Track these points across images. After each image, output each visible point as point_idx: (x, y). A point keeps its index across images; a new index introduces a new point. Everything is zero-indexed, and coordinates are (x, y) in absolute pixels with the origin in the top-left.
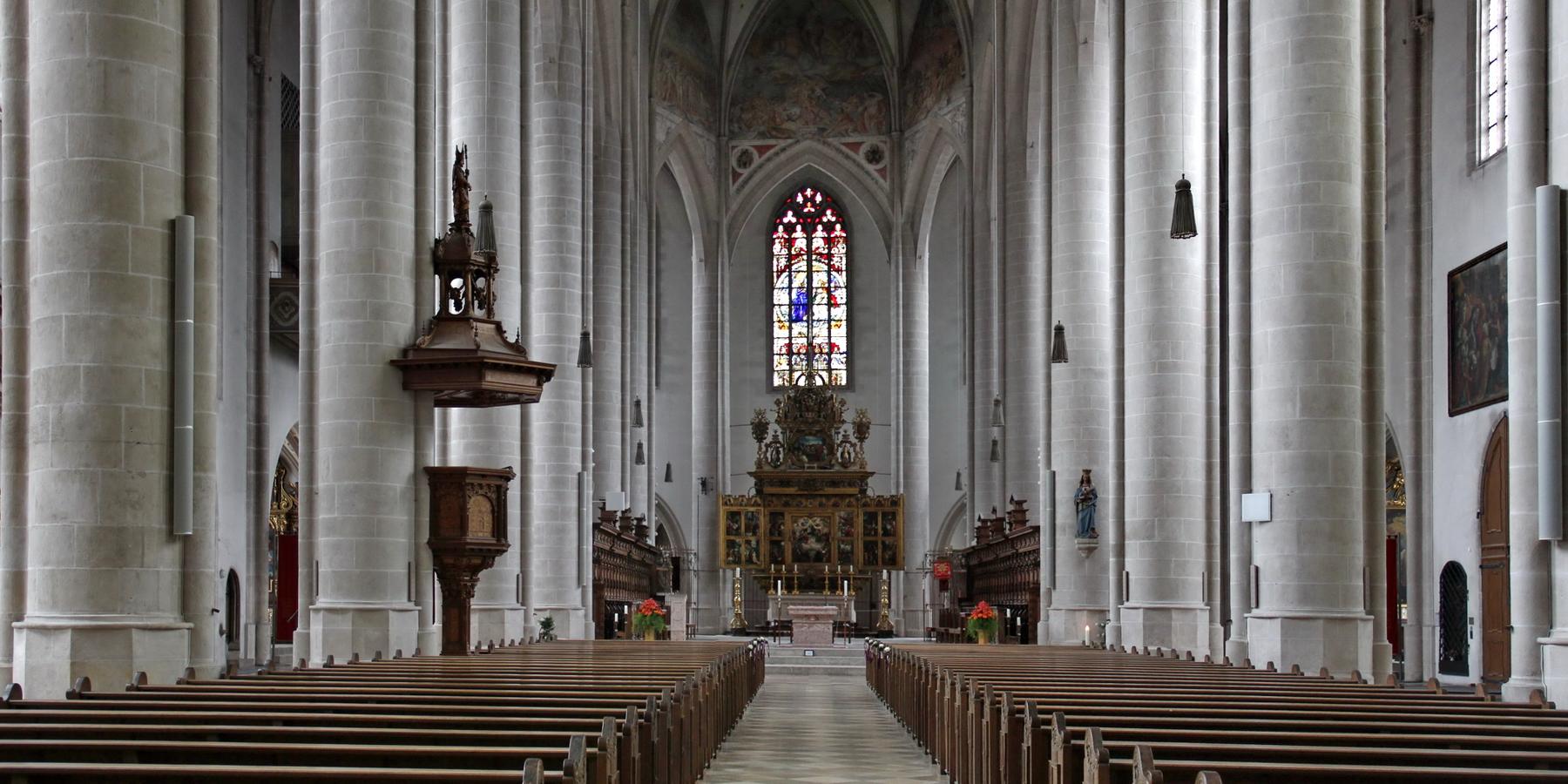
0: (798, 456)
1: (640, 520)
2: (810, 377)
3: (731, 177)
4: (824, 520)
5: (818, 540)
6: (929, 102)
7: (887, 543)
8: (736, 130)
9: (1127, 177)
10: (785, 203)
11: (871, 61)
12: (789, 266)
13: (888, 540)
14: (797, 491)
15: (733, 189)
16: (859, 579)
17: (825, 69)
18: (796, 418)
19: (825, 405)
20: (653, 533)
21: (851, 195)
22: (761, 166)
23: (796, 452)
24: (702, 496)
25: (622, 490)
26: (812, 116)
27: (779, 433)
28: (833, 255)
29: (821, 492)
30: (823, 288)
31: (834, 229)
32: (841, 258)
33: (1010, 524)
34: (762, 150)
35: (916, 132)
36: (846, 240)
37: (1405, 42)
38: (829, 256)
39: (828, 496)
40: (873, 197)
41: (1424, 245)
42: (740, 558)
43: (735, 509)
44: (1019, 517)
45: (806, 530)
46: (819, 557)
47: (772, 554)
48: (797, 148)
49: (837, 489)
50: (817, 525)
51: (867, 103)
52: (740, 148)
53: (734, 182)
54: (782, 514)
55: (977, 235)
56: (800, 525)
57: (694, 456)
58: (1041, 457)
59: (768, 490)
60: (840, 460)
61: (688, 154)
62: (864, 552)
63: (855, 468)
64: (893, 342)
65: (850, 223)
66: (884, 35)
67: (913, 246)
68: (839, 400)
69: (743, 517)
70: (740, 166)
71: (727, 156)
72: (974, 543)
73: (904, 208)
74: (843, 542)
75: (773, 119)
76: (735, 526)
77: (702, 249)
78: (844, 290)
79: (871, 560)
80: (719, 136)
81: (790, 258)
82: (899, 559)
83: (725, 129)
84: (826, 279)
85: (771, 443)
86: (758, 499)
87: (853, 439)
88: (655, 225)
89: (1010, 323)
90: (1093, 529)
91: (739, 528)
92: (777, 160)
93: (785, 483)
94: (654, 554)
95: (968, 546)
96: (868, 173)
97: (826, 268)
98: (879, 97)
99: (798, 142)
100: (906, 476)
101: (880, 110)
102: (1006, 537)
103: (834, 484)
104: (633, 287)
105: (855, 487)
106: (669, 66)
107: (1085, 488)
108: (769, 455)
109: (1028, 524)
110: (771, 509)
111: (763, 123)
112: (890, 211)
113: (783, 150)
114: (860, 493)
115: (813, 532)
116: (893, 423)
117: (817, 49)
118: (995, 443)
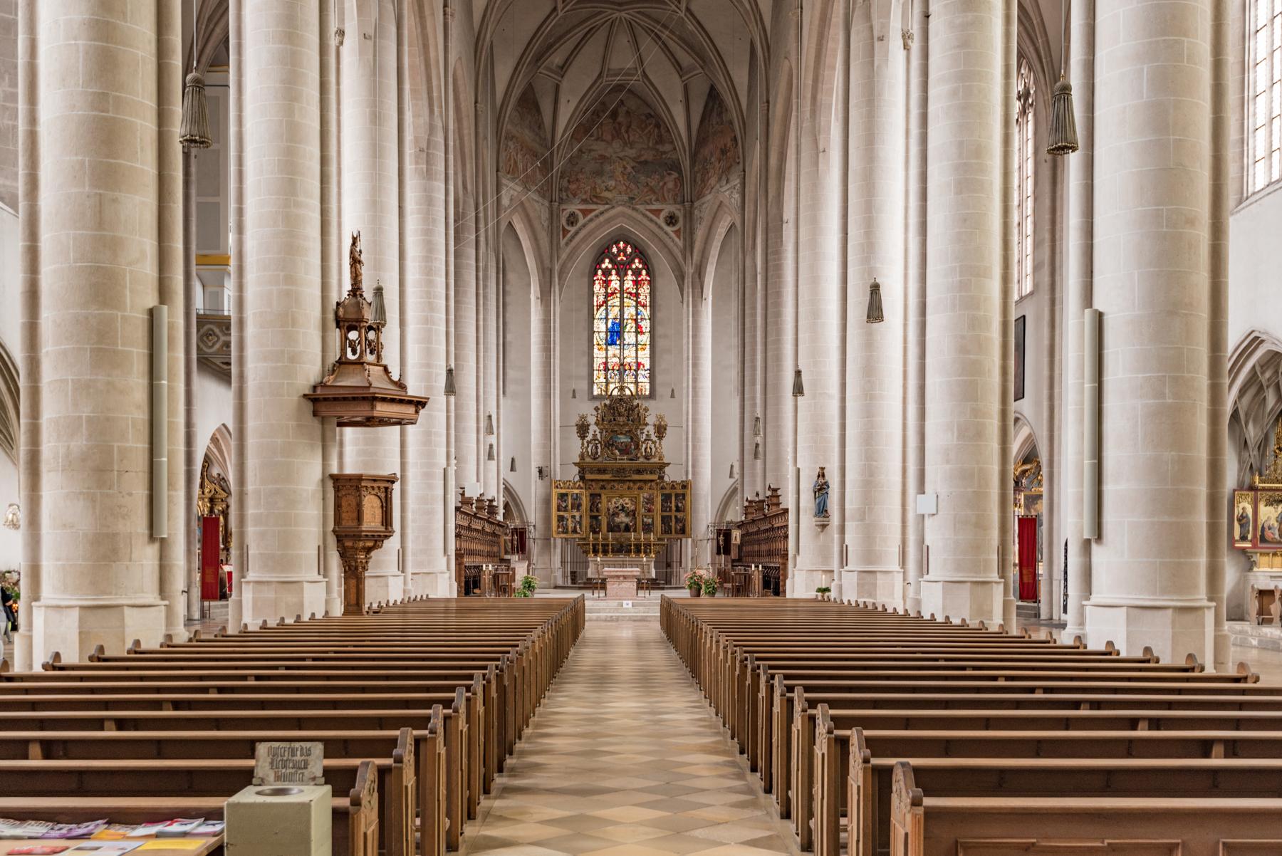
1: (491, 501)
2: (622, 389)
3: (561, 233)
5: (627, 515)
6: (713, 181)
8: (565, 197)
9: (849, 258)
11: (667, 147)
13: (680, 515)
15: (563, 242)
17: (632, 152)
18: (611, 421)
19: (633, 410)
20: (501, 511)
21: (653, 249)
22: (584, 226)
24: (539, 481)
25: (478, 481)
26: (625, 188)
27: (597, 433)
29: (629, 478)
33: (768, 505)
34: (585, 213)
35: (703, 204)
37: (1046, 161)
39: (635, 482)
40: (671, 252)
41: (1057, 308)
42: (567, 529)
43: (564, 491)
44: (774, 500)
45: (617, 507)
46: (627, 529)
47: (591, 526)
48: (613, 212)
51: (667, 179)
52: (569, 211)
53: (564, 237)
54: (600, 495)
55: (748, 284)
57: (532, 450)
58: (790, 457)
59: (588, 476)
61: (527, 216)
63: (656, 460)
64: (685, 363)
66: (677, 128)
68: (644, 407)
70: (568, 224)
71: (558, 216)
72: (743, 518)
73: (694, 261)
74: (646, 516)
75: (594, 189)
76: (564, 505)
77: (538, 289)
79: (667, 530)
80: (551, 201)
83: (556, 196)
85: (591, 440)
86: (581, 483)
87: (654, 438)
88: (502, 271)
89: (770, 354)
90: (826, 511)
91: (567, 506)
92: (597, 221)
93: (602, 471)
94: (503, 526)
95: (739, 520)
96: (666, 233)
98: (675, 175)
99: (613, 207)
100: (693, 466)
101: (676, 185)
102: (764, 515)
103: (639, 472)
104: (485, 320)
106: (512, 147)
107: (821, 480)
108: (589, 449)
109: (781, 507)
110: (591, 491)
111: (586, 192)
113: (602, 213)
114: (659, 479)
115: (623, 509)
116: (684, 426)
117: (626, 136)
118: (757, 445)
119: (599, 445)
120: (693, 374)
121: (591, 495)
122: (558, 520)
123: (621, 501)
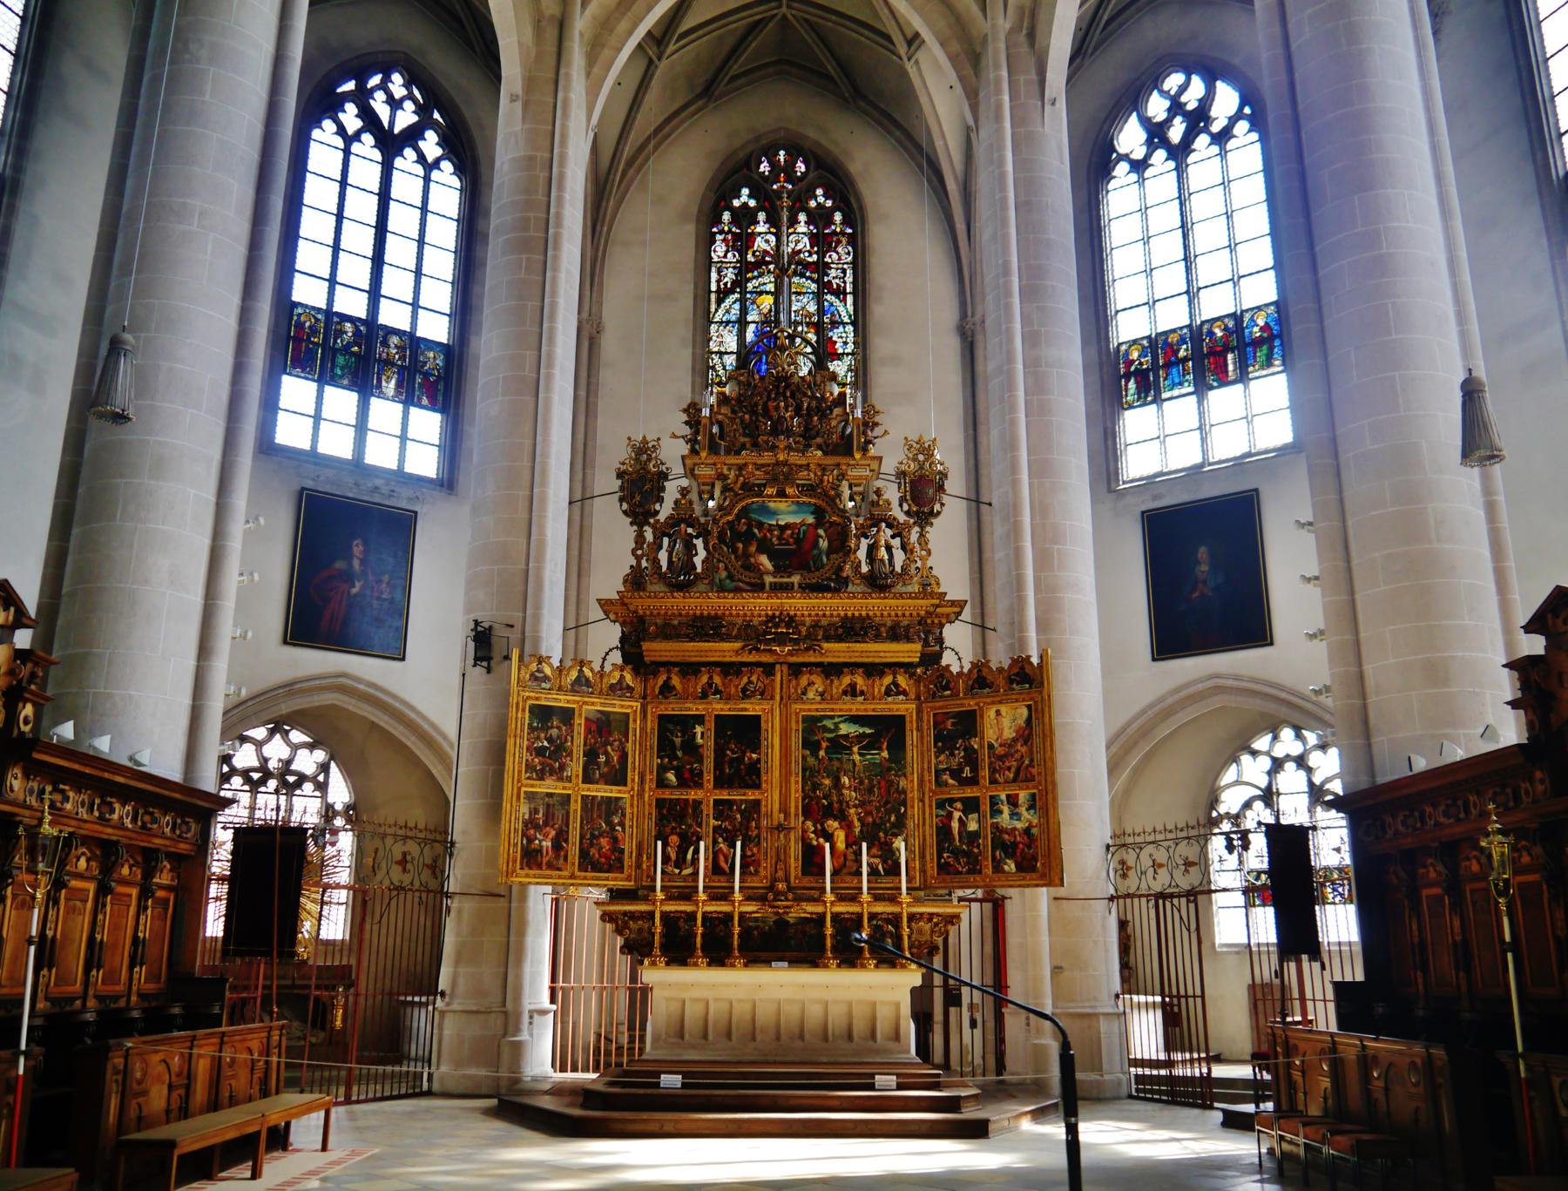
0: (746, 555)
10: (735, 171)
12: (740, 283)
14: (737, 652)
23: (740, 545)
28: (827, 266)
29: (811, 658)
30: (808, 324)
31: (831, 222)
32: (844, 271)
36: (852, 240)
38: (821, 268)
49: (859, 647)
59: (656, 649)
60: (865, 569)
65: (862, 208)
67: (1034, 76)
78: (850, 328)
81: (744, 269)
84: (812, 308)
85: (674, 521)
86: (628, 678)
87: (902, 518)
93: (707, 627)
97: (814, 287)
100: (1043, 626)
105: (909, 640)
108: (663, 556)
112: (980, 15)
119: (699, 543)
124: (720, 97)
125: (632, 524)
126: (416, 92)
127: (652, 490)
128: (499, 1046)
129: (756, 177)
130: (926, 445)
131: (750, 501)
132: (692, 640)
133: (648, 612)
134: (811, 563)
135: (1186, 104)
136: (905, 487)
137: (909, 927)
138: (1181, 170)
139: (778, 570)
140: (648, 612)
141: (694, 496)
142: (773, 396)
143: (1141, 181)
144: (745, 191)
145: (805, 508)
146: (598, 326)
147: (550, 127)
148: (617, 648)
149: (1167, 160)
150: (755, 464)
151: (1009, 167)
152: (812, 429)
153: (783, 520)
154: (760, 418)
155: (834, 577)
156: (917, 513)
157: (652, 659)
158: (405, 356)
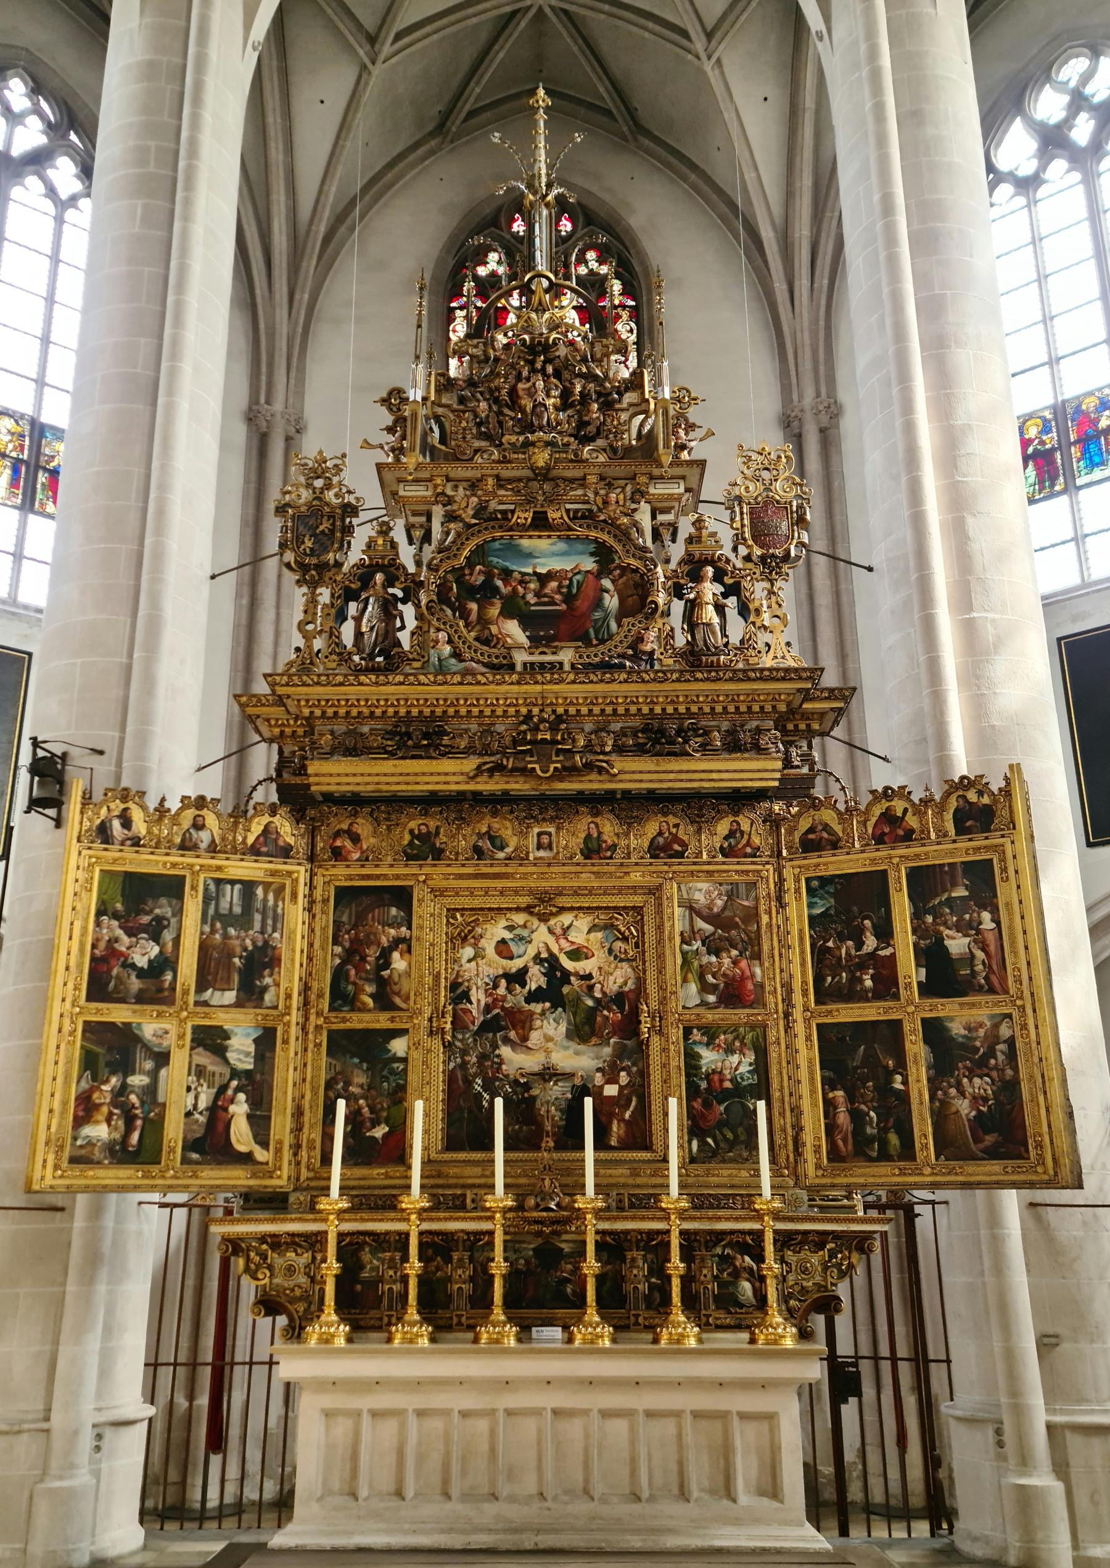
0: (484, 622)
4: (609, 927)
7: (957, 1029)
16: (819, 1240)
19: (608, 405)
23: (474, 606)
27: (399, 534)
29: (592, 784)
42: (155, 1126)
45: (518, 978)
50: (576, 954)
54: (402, 897)
56: (489, 946)
62: (829, 1084)
69: (193, 906)
74: (711, 1034)
76: (144, 953)
82: (1035, 1120)
91: (165, 963)
120: (922, 281)
121: (345, 895)
122: (89, 1062)
123: (542, 937)
124: (458, 136)
125: (298, 583)
126: (44, 104)
127: (332, 531)
128: (31, 1498)
129: (508, 237)
130: (773, 456)
131: (489, 537)
132: (392, 755)
133: (318, 712)
134: (592, 631)
135: (1093, 96)
136: (742, 519)
137: (782, 1260)
138: (1090, 182)
139: (536, 642)
140: (318, 712)
141: (399, 534)
142: (525, 373)
143: (1031, 204)
144: (493, 257)
145: (580, 547)
146: (298, 421)
147: (183, 23)
148: (271, 779)
149: (1068, 171)
150: (498, 477)
151: (886, 61)
152: (588, 423)
153: (543, 565)
154: (506, 411)
155: (630, 652)
156: (763, 558)
157: (325, 788)
158: (22, 447)
